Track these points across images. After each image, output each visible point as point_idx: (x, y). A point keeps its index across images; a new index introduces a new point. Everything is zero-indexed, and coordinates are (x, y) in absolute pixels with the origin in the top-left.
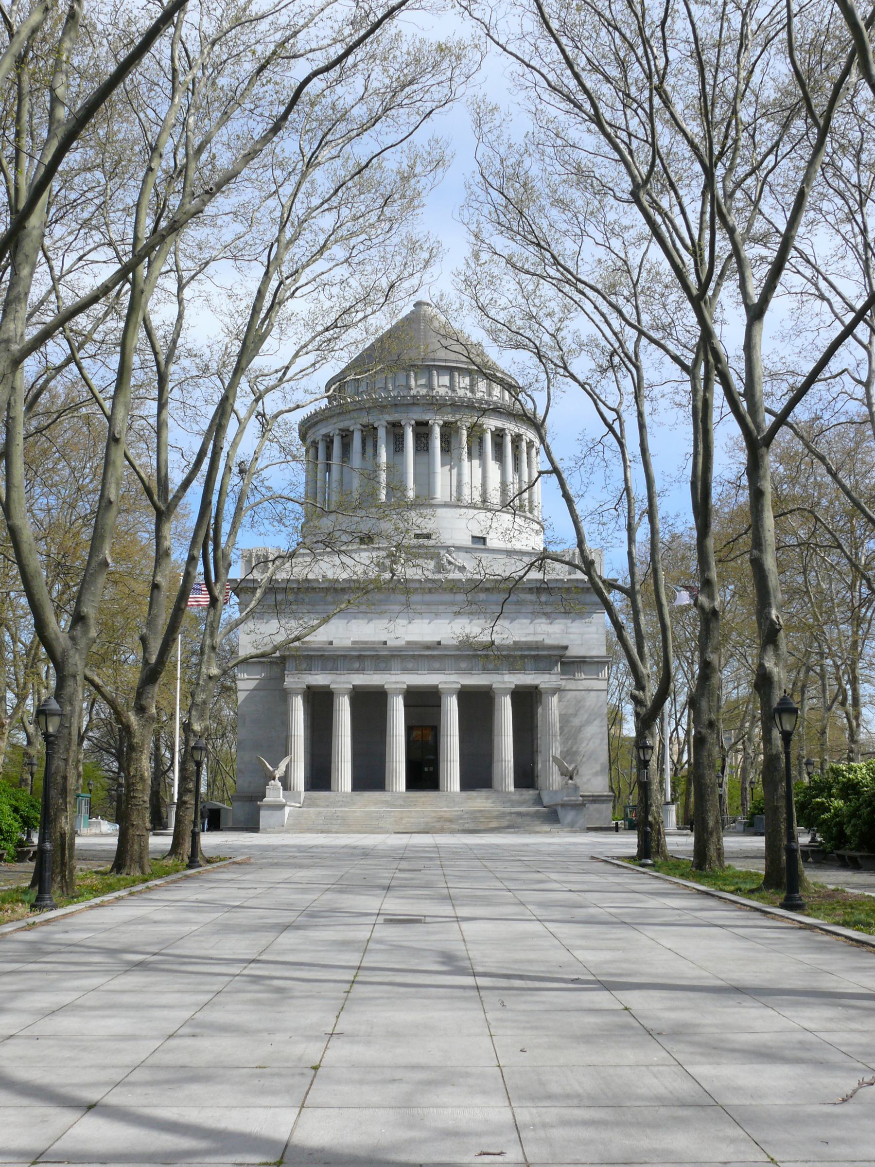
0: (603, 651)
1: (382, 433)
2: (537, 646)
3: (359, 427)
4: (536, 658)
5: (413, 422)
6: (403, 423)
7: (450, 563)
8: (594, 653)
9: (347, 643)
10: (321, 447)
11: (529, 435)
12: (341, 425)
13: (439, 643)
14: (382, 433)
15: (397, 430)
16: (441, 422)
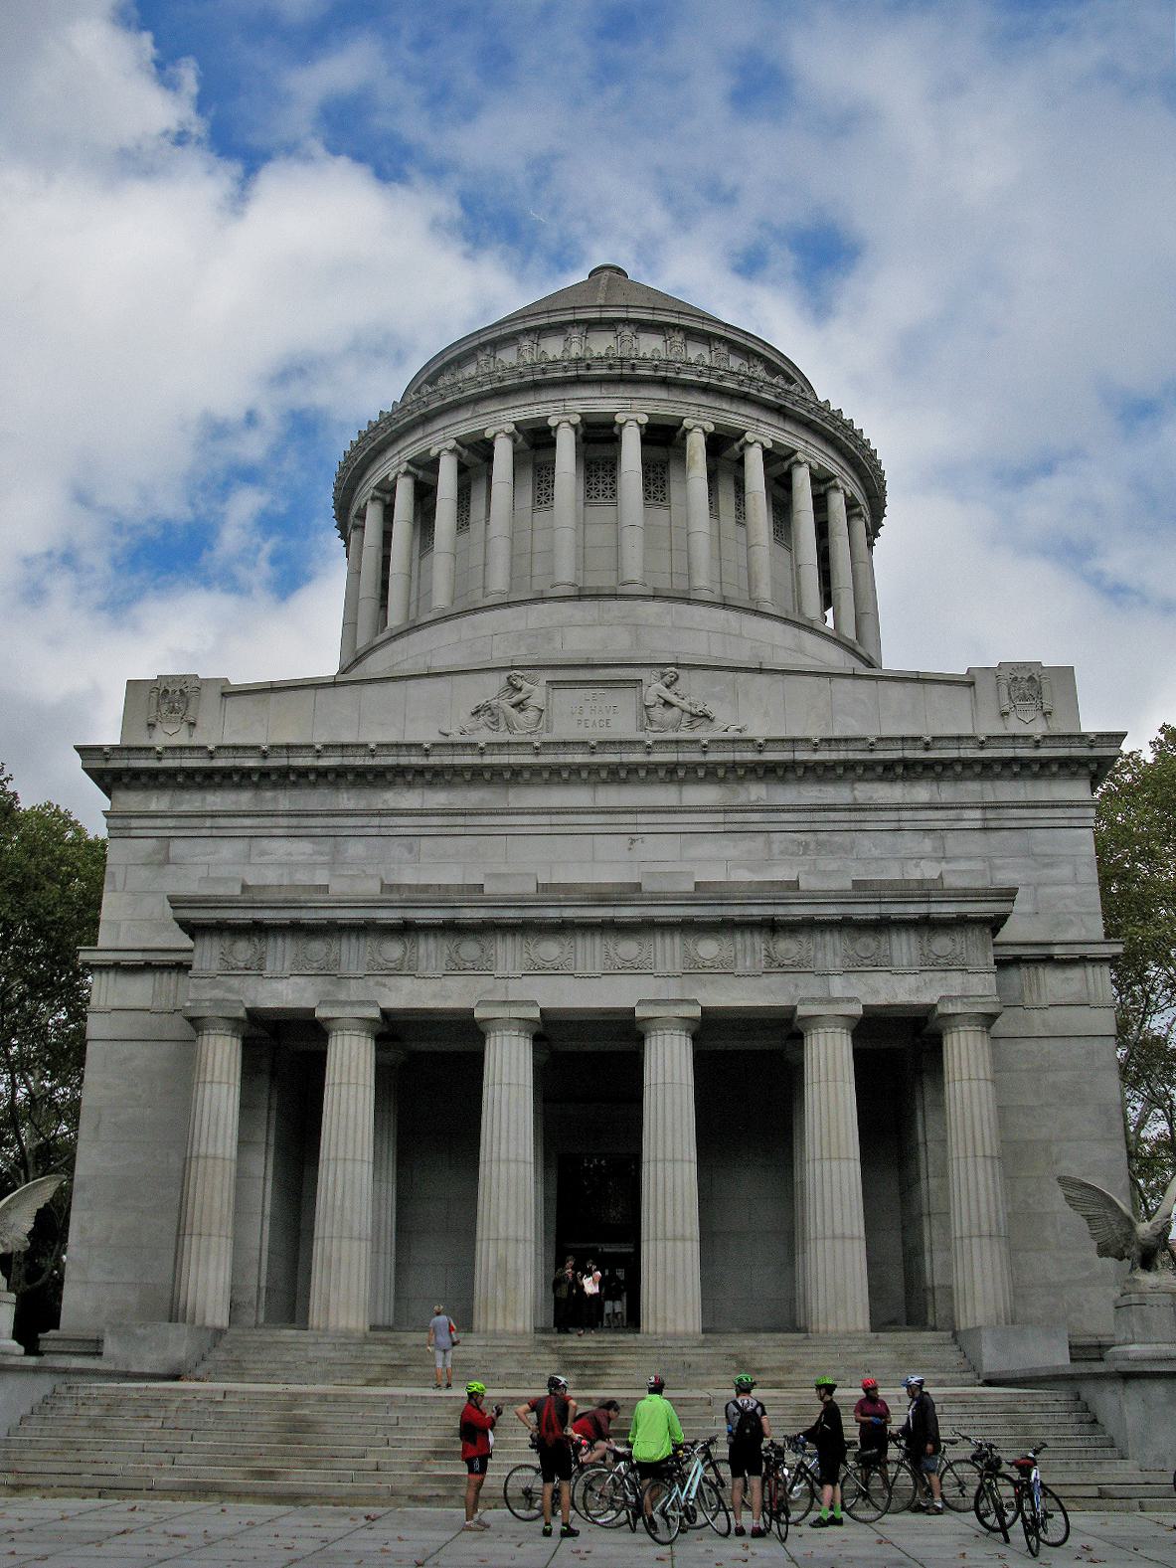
0: (1096, 928)
1: (503, 452)
2: (925, 891)
3: (452, 444)
4: (927, 925)
5: (577, 419)
6: (552, 422)
7: (667, 704)
8: (1069, 937)
9: (371, 888)
10: (373, 514)
11: (848, 484)
12: (412, 452)
13: (637, 887)
14: (503, 452)
15: (542, 457)
16: (644, 420)
